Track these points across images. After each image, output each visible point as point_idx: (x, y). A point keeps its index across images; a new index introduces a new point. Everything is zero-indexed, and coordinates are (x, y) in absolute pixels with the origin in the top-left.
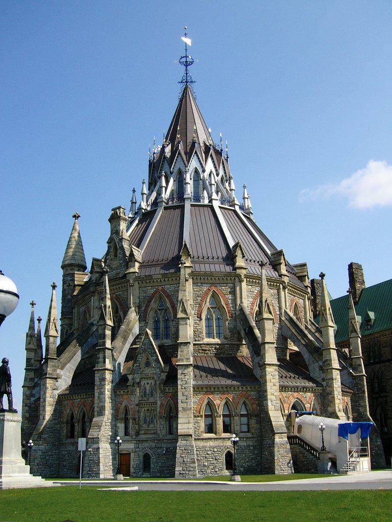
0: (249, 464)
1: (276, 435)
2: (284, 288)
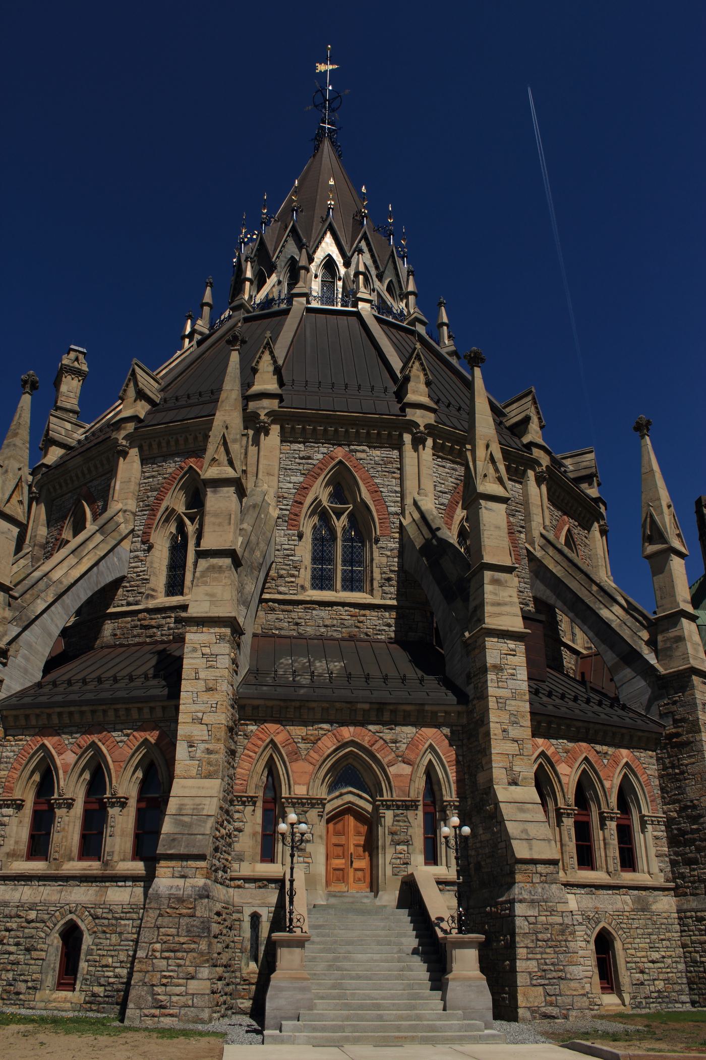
1: (163, 863)
2: (418, 442)
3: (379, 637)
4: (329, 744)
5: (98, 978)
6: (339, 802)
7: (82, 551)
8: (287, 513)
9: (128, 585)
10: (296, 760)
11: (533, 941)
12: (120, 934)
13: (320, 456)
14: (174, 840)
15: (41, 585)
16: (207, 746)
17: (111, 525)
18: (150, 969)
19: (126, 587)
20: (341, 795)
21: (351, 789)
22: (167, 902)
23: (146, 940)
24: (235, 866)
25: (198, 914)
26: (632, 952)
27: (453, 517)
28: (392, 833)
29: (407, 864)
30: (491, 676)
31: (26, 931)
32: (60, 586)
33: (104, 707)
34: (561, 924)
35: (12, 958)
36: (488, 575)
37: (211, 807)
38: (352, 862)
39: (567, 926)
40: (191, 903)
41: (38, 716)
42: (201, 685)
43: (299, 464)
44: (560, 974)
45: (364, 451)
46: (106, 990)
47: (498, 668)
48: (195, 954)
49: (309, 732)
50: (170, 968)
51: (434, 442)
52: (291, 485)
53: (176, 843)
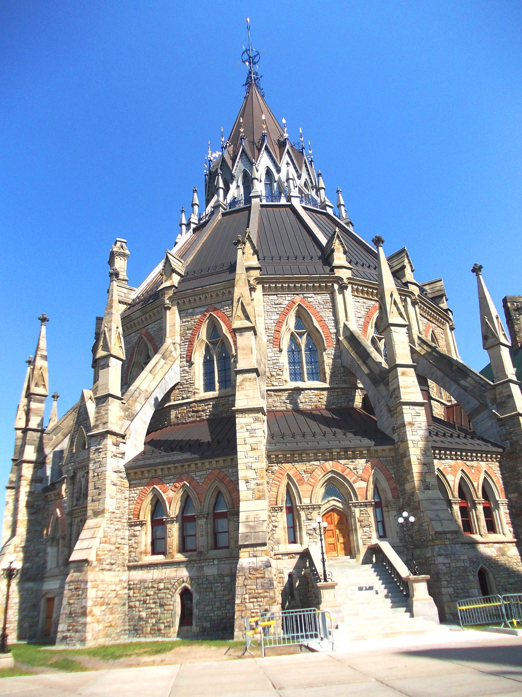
0: (220, 613)
1: (243, 550)
2: (343, 288)
3: (333, 407)
4: (319, 473)
5: (205, 618)
6: (327, 506)
7: (155, 370)
8: (272, 338)
9: (181, 387)
10: (303, 484)
11: (449, 577)
12: (215, 592)
13: (287, 302)
14: (247, 536)
15: (137, 394)
16: (256, 481)
17: (168, 353)
18: (244, 609)
19: (180, 388)
20: (329, 501)
21: (334, 498)
22: (248, 571)
23: (240, 593)
24: (276, 547)
25: (267, 576)
26: (499, 579)
27: (366, 332)
28: (360, 521)
29: (370, 538)
30: (408, 429)
31: (159, 595)
32: (147, 393)
33: (189, 463)
34: (463, 567)
35: (153, 611)
36: (400, 370)
37: (264, 515)
38: (338, 539)
39: (467, 567)
40: (262, 570)
41: (149, 471)
42: (248, 447)
43: (275, 308)
44: (466, 594)
45: (311, 297)
46: (211, 624)
47: (411, 424)
48: (268, 599)
49: (308, 468)
50: (255, 607)
51: (352, 287)
52: (272, 322)
53: (248, 538)
